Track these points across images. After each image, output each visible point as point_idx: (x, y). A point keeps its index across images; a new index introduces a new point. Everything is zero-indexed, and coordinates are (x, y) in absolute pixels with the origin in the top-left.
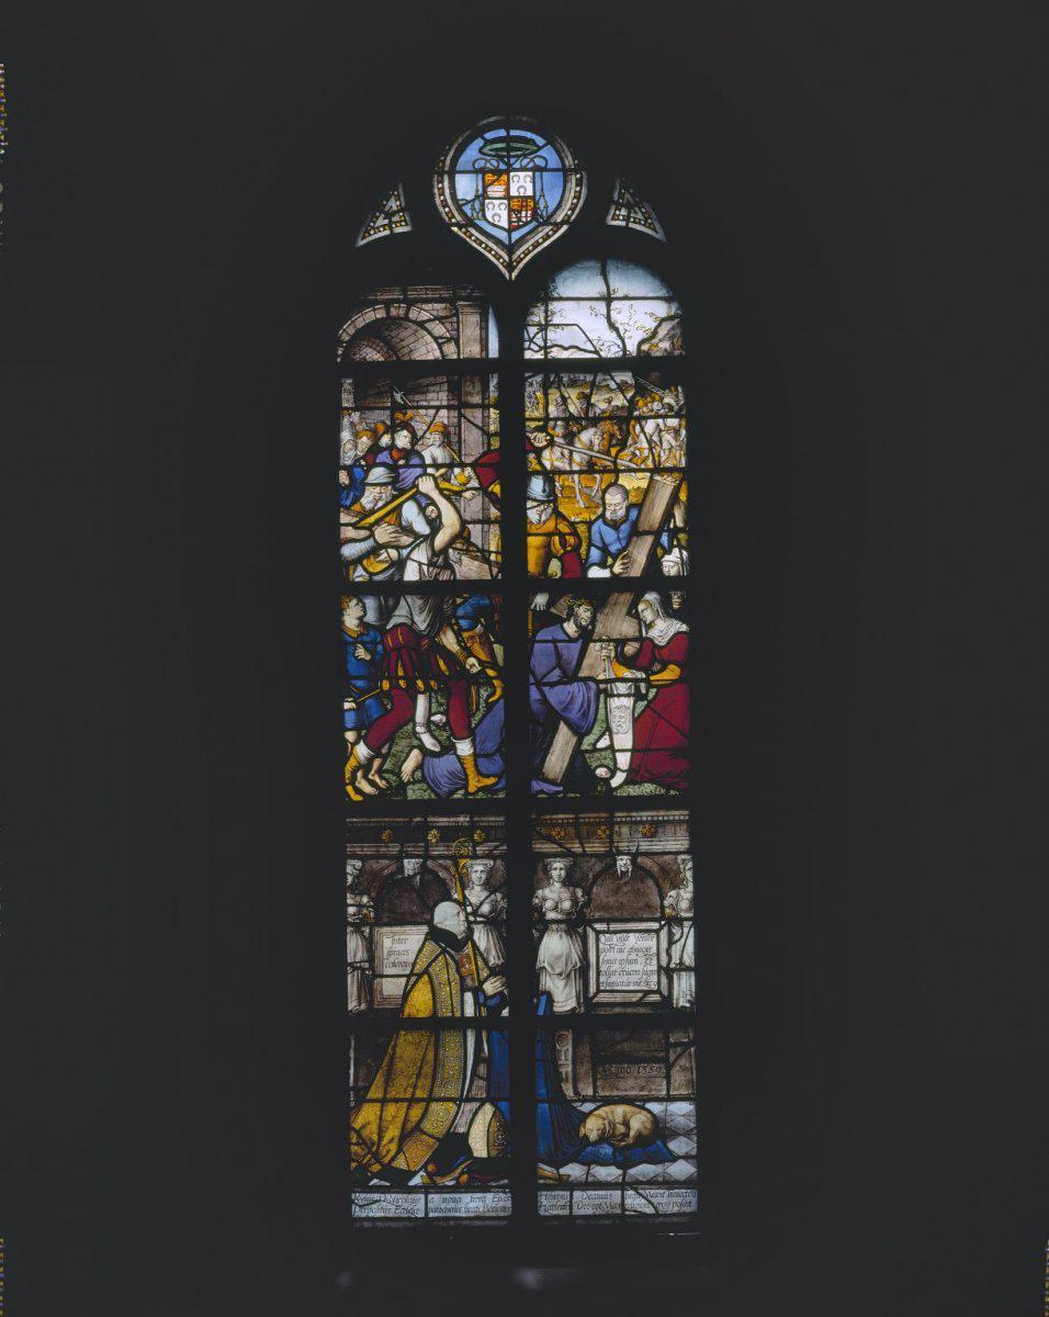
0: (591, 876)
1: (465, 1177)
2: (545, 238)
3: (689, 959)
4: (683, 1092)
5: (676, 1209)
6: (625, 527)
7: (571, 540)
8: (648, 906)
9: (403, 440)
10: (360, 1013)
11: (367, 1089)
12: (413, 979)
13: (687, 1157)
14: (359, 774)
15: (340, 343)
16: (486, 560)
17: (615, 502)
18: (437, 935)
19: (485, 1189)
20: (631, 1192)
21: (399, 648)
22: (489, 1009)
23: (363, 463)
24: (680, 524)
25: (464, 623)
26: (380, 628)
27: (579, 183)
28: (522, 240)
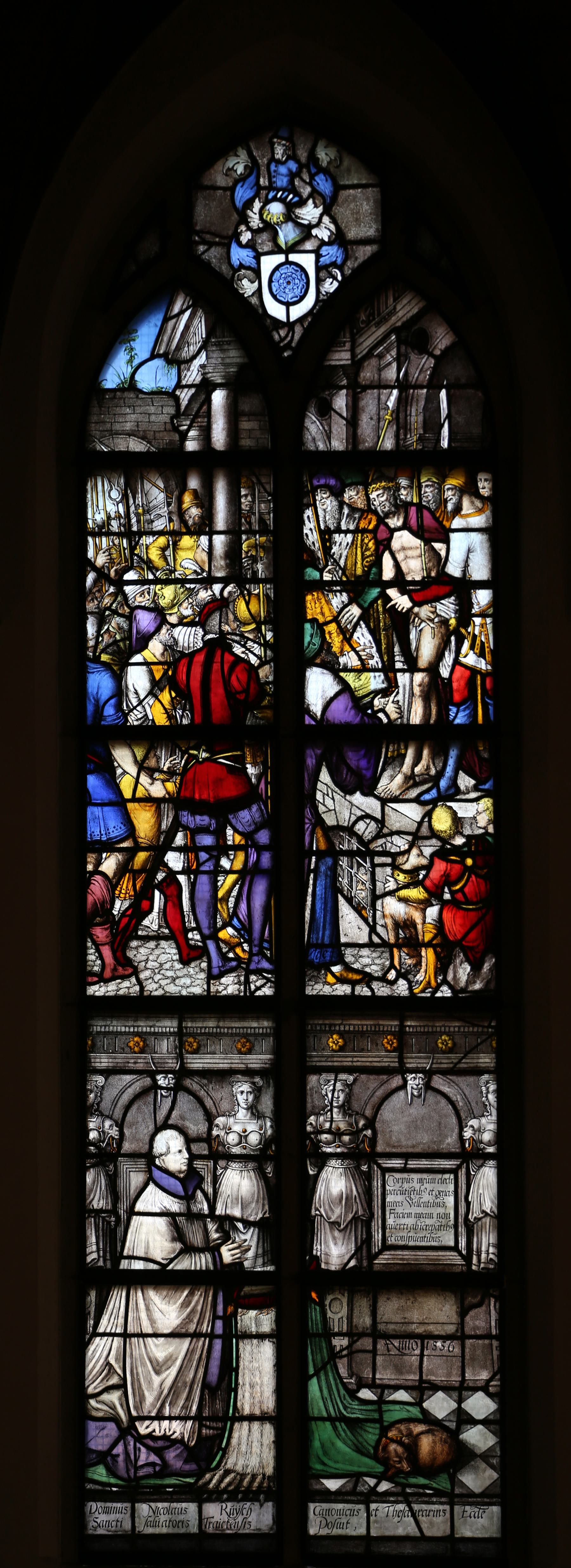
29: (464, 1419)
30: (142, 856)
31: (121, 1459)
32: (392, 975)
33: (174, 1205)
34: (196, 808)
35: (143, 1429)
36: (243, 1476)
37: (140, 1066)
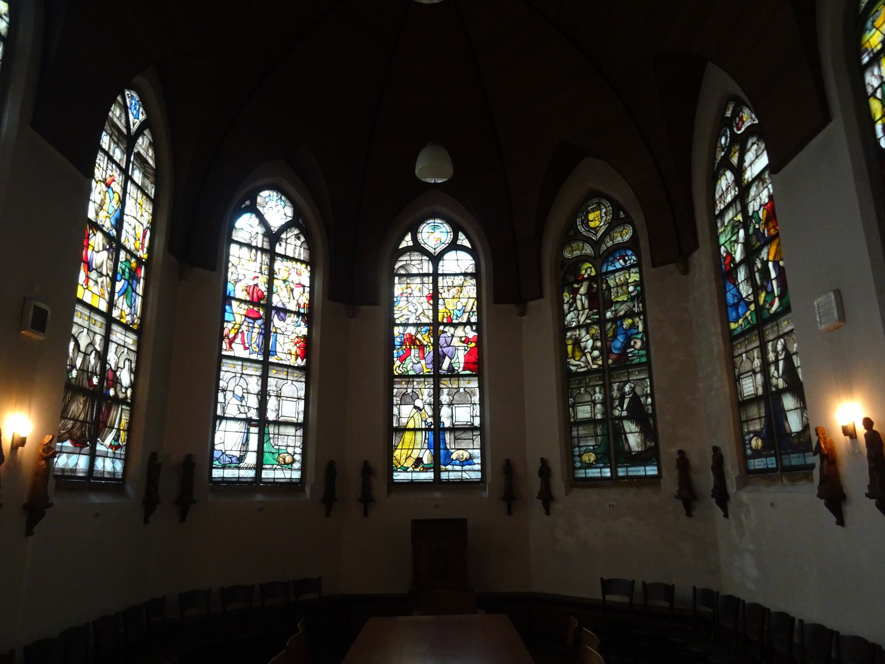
0: (454, 393)
1: (422, 469)
2: (443, 247)
3: (478, 414)
4: (477, 447)
5: (475, 477)
6: (462, 311)
7: (449, 314)
8: (468, 401)
9: (409, 291)
10: (396, 427)
11: (397, 446)
12: (410, 418)
13: (478, 464)
14: (397, 368)
15: (394, 269)
16: (429, 318)
17: (460, 306)
18: (415, 407)
19: (427, 472)
20: (464, 473)
21: (407, 339)
22: (428, 426)
23: (400, 296)
24: (475, 310)
25: (423, 333)
26: (403, 334)
27: (451, 235)
28: (437, 247)
29: (295, 453)
30: (237, 326)
31: (222, 460)
32: (286, 360)
33: (239, 403)
34: (250, 318)
35: (227, 453)
36: (249, 464)
37: (233, 371)
